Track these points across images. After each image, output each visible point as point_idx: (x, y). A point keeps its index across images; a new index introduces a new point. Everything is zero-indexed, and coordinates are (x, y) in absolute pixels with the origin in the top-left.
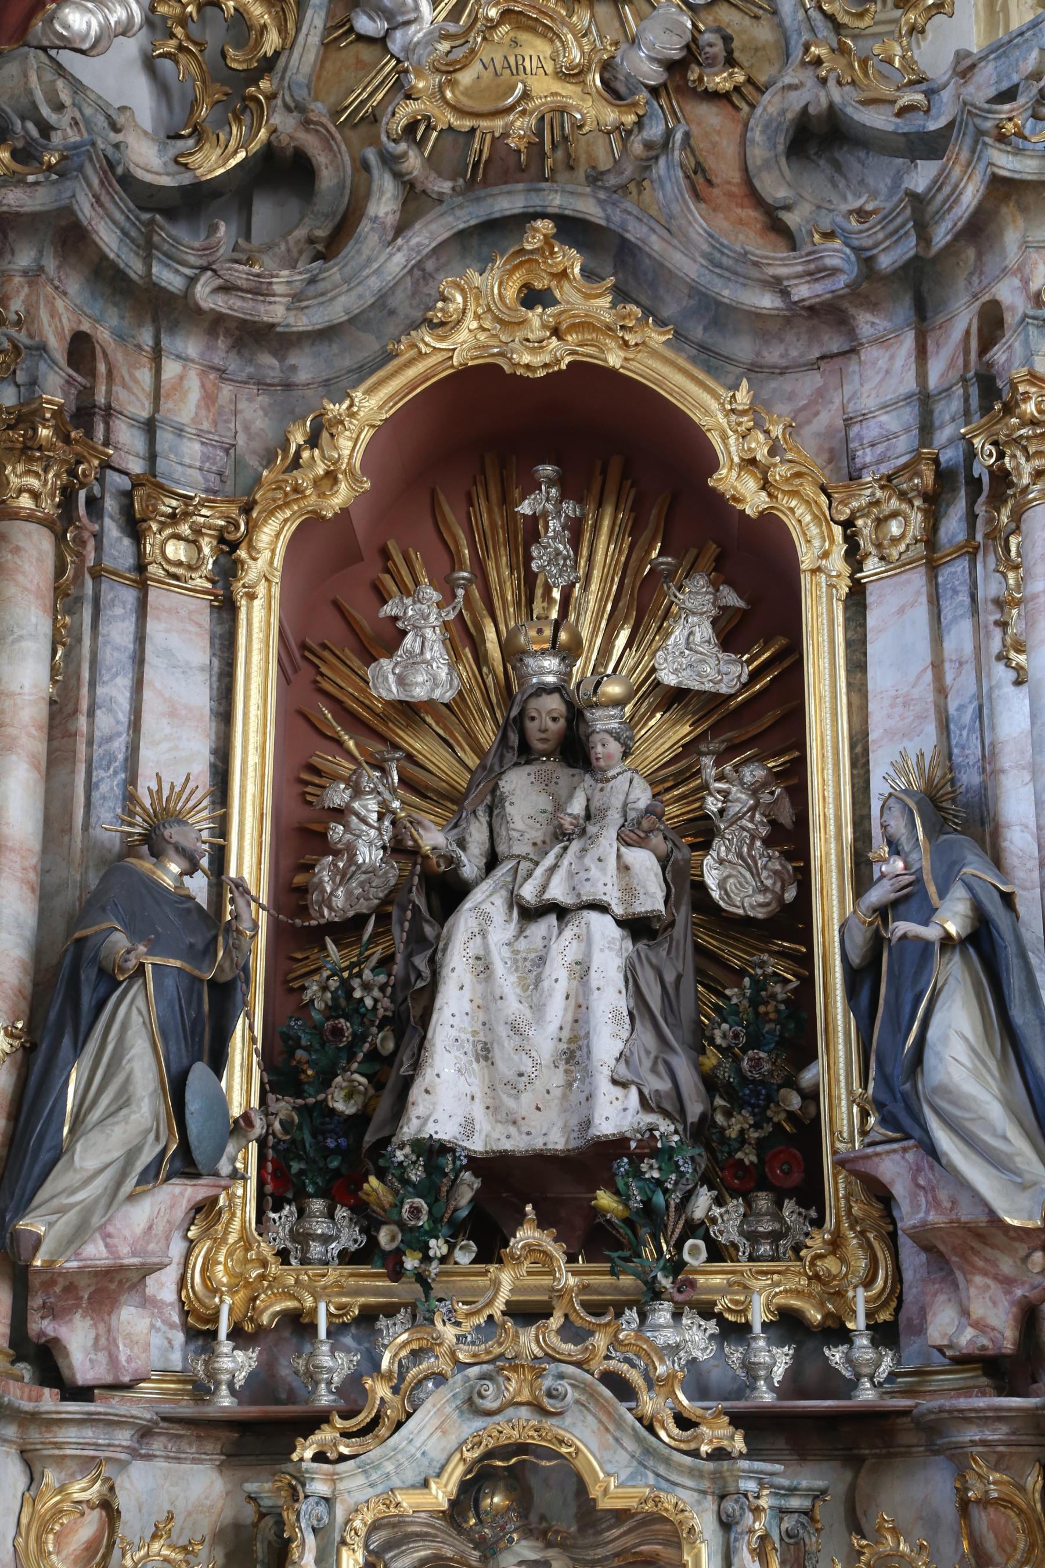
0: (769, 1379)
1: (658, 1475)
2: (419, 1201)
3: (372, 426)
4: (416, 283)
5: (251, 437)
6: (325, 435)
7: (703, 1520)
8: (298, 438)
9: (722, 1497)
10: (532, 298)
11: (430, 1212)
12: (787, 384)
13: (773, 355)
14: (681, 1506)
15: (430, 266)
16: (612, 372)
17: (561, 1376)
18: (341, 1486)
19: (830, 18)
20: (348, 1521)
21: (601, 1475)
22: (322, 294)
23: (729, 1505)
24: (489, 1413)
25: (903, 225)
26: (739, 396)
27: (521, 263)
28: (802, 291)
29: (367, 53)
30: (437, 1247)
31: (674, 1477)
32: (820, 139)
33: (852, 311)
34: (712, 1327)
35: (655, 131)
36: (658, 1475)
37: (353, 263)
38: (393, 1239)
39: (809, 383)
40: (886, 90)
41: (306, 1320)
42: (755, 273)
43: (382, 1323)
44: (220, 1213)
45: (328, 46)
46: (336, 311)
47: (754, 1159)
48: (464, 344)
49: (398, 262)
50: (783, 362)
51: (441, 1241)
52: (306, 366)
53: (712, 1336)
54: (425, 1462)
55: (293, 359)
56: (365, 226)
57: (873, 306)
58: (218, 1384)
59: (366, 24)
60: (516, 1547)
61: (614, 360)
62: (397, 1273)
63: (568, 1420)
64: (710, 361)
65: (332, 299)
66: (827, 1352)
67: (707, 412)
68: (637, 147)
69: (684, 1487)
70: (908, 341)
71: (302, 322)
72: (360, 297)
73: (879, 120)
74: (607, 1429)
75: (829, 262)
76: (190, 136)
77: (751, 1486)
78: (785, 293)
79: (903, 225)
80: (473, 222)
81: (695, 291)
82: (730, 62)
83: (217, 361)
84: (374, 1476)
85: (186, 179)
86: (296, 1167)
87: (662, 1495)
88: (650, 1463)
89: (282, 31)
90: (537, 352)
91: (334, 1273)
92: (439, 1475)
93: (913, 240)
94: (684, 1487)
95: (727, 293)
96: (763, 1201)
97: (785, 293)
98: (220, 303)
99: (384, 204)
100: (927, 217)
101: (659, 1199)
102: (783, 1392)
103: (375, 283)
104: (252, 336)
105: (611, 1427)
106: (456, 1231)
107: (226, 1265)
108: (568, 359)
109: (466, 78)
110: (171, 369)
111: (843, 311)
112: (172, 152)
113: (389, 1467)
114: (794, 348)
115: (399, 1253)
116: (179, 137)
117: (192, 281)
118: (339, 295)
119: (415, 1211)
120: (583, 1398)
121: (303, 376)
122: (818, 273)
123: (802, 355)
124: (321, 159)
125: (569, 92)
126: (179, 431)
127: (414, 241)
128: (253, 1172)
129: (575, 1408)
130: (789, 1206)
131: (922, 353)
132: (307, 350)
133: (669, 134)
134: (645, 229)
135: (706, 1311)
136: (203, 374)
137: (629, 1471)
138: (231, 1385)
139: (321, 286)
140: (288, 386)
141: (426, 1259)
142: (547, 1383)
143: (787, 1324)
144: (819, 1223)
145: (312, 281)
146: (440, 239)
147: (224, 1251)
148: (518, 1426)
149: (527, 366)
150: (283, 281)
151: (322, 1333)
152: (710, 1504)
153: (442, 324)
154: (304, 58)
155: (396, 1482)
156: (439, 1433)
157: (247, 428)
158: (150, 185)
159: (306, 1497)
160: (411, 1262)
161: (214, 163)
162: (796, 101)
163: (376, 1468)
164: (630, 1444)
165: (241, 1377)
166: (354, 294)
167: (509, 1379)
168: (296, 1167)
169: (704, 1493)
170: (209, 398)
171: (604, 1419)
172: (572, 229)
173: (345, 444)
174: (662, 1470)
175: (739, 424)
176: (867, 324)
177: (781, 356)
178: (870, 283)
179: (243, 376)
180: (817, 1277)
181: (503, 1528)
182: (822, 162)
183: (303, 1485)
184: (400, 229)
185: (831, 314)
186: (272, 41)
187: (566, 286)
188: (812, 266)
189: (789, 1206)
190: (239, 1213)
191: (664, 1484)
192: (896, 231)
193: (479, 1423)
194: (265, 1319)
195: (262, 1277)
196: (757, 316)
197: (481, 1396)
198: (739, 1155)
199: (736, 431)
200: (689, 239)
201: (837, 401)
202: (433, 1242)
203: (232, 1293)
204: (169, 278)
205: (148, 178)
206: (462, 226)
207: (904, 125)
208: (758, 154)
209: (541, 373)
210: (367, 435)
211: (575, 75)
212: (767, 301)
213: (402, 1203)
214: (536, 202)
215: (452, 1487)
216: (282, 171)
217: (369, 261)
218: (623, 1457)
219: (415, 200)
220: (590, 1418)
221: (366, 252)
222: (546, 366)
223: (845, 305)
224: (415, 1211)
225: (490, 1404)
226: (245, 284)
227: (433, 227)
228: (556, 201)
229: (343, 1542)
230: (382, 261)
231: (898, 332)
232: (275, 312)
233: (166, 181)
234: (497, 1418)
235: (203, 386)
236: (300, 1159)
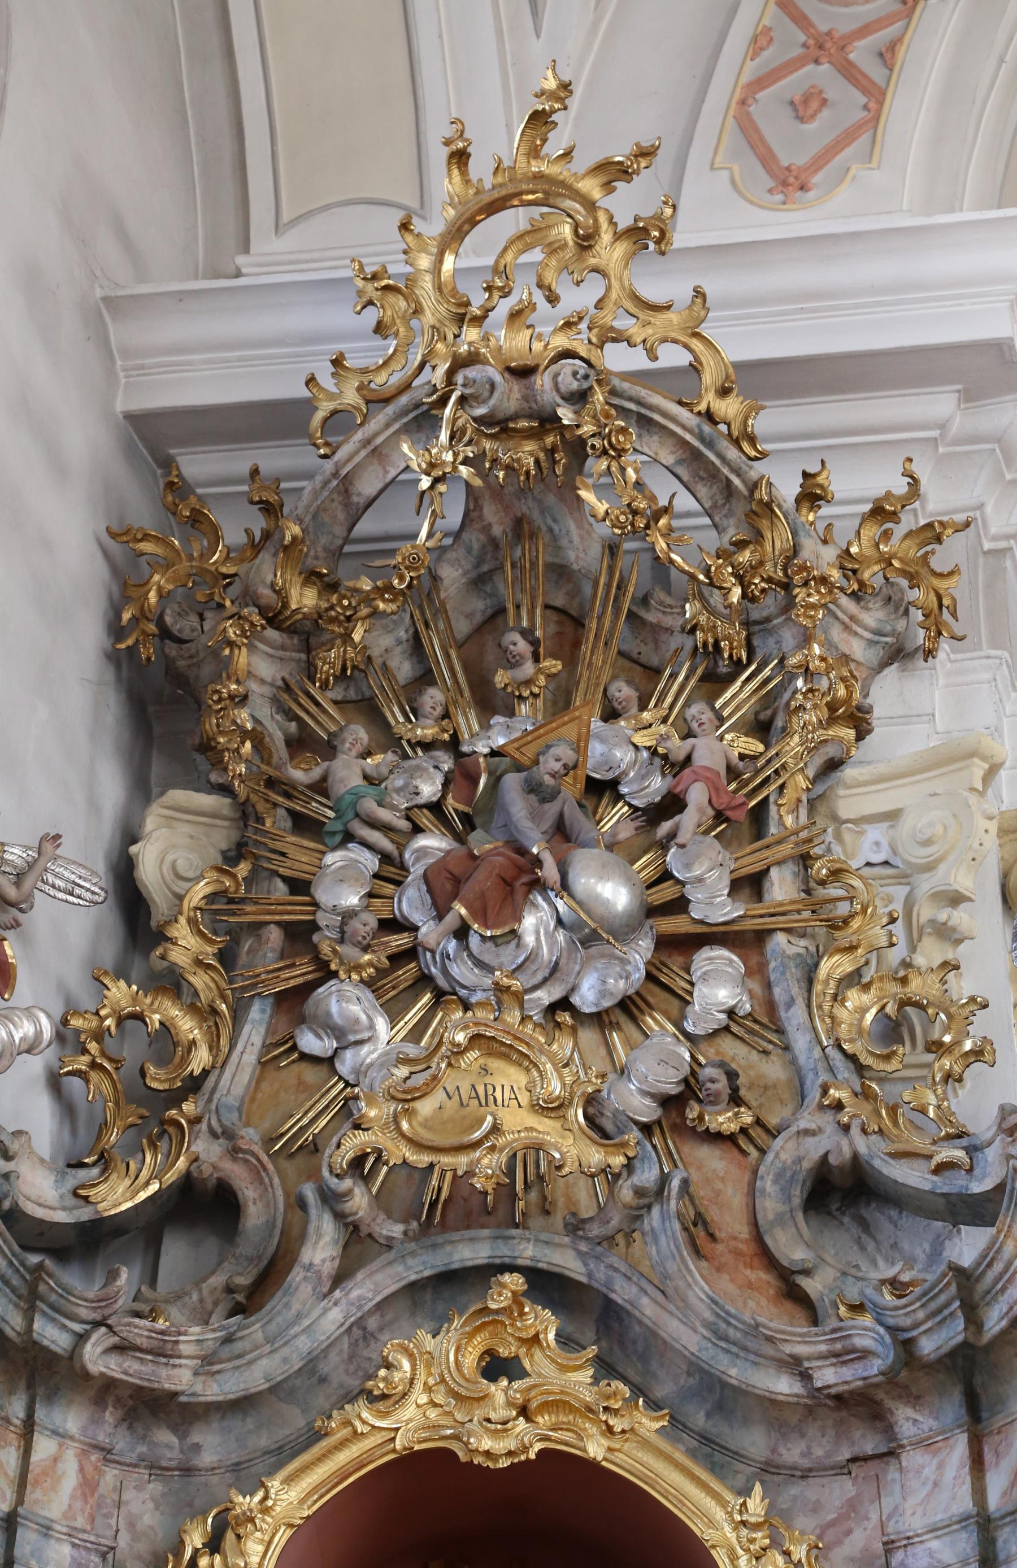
3: (290, 1526)
4: (354, 1344)
5: (135, 1537)
6: (230, 1536)
8: (195, 1539)
10: (496, 1367)
12: (811, 1490)
13: (792, 1453)
15: (372, 1323)
16: (592, 1467)
19: (852, 1058)
22: (239, 1356)
25: (948, 1304)
26: (751, 1504)
27: (484, 1325)
28: (827, 1376)
29: (310, 1074)
32: (841, 1192)
33: (889, 1403)
35: (647, 1176)
37: (279, 1319)
39: (838, 1491)
40: (920, 1143)
42: (769, 1350)
45: (266, 1064)
46: (254, 1378)
48: (410, 1423)
49: (333, 1318)
50: (806, 1463)
52: (212, 1445)
55: (195, 1437)
56: (297, 1275)
57: (915, 1399)
59: (310, 1042)
61: (595, 1449)
64: (714, 1455)
65: (250, 1363)
67: (712, 1523)
68: (626, 1193)
70: (960, 1447)
71: (212, 1391)
72: (285, 1360)
73: (912, 1176)
75: (860, 1342)
76: (95, 1164)
78: (805, 1376)
79: (948, 1304)
80: (427, 1273)
81: (696, 1368)
82: (736, 1100)
83: (102, 1437)
85: (85, 1214)
89: (214, 1047)
90: (499, 1437)
93: (960, 1324)
95: (735, 1372)
97: (805, 1376)
98: (113, 1367)
99: (321, 1249)
100: (977, 1297)
103: (304, 1344)
104: (148, 1407)
108: (538, 1446)
109: (425, 1107)
110: (43, 1447)
111: (879, 1403)
112: (71, 1183)
114: (815, 1445)
116: (81, 1165)
117: (81, 1338)
118: (260, 1357)
121: (207, 1458)
122: (846, 1355)
123: (828, 1455)
124: (248, 1192)
125: (546, 1128)
126: (46, 1530)
127: (355, 1294)
131: (977, 1463)
132: (215, 1425)
133: (664, 1180)
134: (634, 1290)
136: (83, 1454)
139: (238, 1346)
140: (187, 1471)
145: (228, 1340)
146: (386, 1292)
149: (487, 1453)
150: (193, 1338)
153: (384, 1397)
154: (237, 1078)
157: (131, 1525)
158: (42, 1222)
161: (119, 1196)
162: (814, 1149)
166: (277, 1357)
170: (88, 1485)
172: (546, 1286)
173: (254, 1548)
175: (752, 1541)
176: (909, 1421)
177: (803, 1455)
178: (909, 1372)
179: (132, 1457)
182: (846, 1220)
184: (339, 1279)
185: (862, 1405)
186: (201, 1059)
187: (538, 1354)
188: (838, 1346)
192: (939, 1311)
196: (771, 1403)
199: (747, 1551)
200: (689, 1304)
201: (874, 1517)
204: (53, 1335)
205: (39, 1213)
206: (413, 1277)
207: (943, 1184)
208: (770, 1206)
209: (504, 1463)
210: (283, 1536)
211: (553, 1109)
212: (785, 1386)
214: (503, 1252)
216: (202, 1206)
217: (299, 1316)
219: (358, 1245)
221: (296, 1306)
222: (510, 1453)
223: (880, 1395)
226: (145, 1346)
227: (379, 1277)
228: (527, 1252)
230: (313, 1317)
231: (947, 1433)
232: (180, 1378)
233: (61, 1217)
235: (81, 1470)
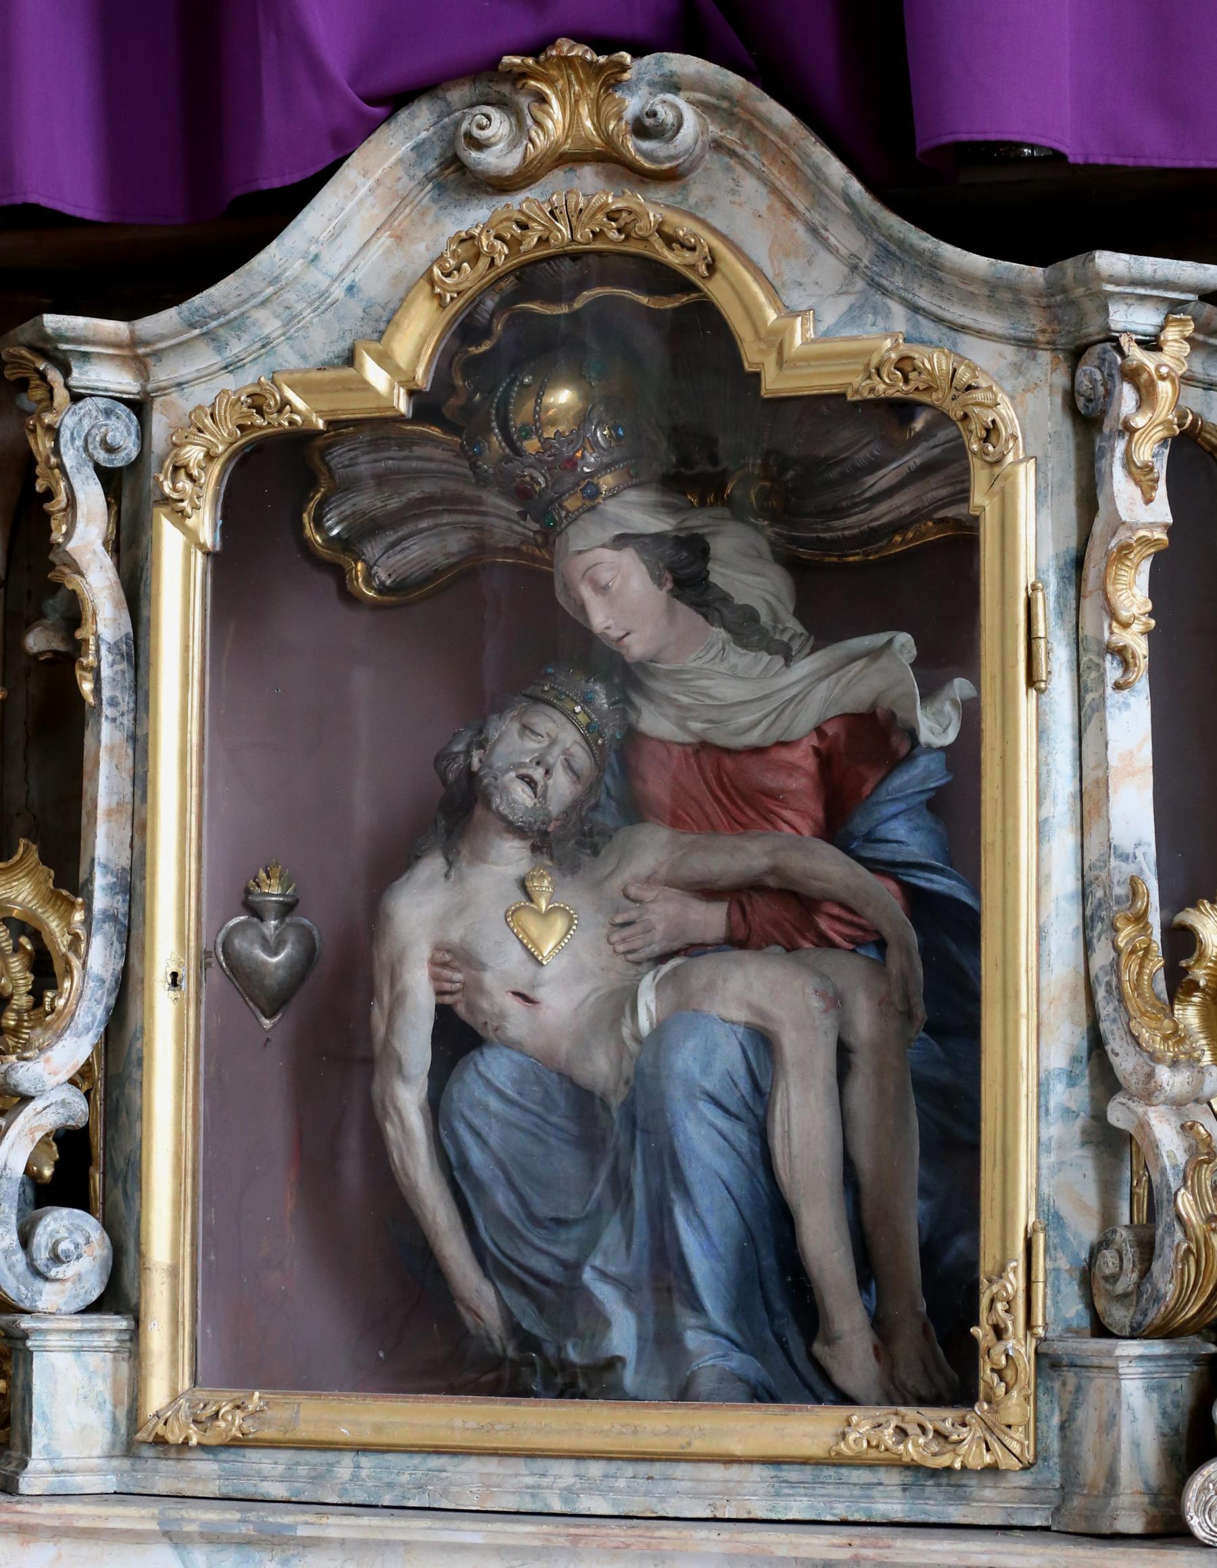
1: (916, 309)
7: (1017, 404)
9: (1076, 355)
14: (964, 376)
18: (162, 374)
21: (771, 315)
24: (501, 185)
31: (955, 312)
36: (916, 309)
54: (355, 308)
60: (610, 507)
69: (980, 333)
74: (790, 207)
84: (236, 348)
87: (920, 355)
88: (897, 281)
94: (980, 333)
105: (800, 203)
113: (268, 323)
129: (712, 160)
137: (844, 303)
142: (633, 104)
152: (1047, 373)
156: (385, 240)
159: (76, 398)
164: (844, 237)
167: (542, 99)
169: (1028, 344)
171: (782, 182)
174: (924, 298)
183: (66, 372)
191: (930, 330)
193: (476, 215)
218: (829, 269)
220: (750, 184)
225: (500, 157)
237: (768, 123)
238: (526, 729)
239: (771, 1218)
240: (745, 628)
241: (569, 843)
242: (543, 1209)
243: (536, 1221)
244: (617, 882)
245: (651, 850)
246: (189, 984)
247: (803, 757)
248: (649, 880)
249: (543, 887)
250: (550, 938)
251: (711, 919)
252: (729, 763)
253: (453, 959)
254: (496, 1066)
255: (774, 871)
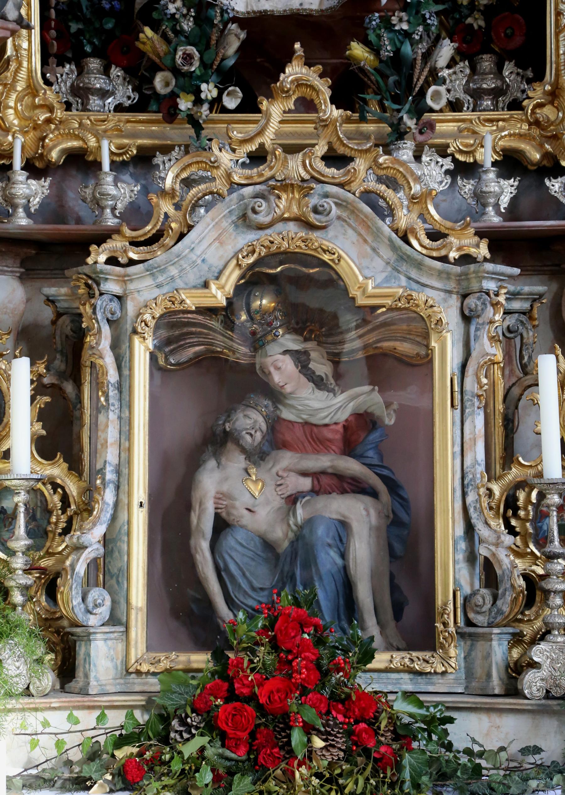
0: (497, 206)
1: (410, 278)
2: (192, 49)
7: (449, 313)
9: (464, 296)
11: (201, 59)
14: (431, 302)
17: (326, 195)
18: (131, 287)
20: (139, 314)
21: (361, 278)
23: (471, 301)
24: (261, 227)
30: (209, 91)
31: (424, 280)
34: (448, 164)
36: (410, 278)
38: (167, 84)
41: (91, 158)
43: (159, 159)
44: (8, 61)
47: (482, 23)
51: (211, 86)
53: (447, 172)
54: (205, 267)
58: (15, 207)
60: (281, 340)
62: (171, 114)
63: (331, 232)
66: (547, 182)
69: (432, 288)
74: (365, 241)
77: (491, 285)
84: (161, 279)
86: (74, 27)
87: (414, 294)
88: (404, 267)
91: (115, 118)
92: (217, 278)
94: (432, 288)
96: (486, 63)
101: (407, 49)
102: (513, 212)
105: (369, 239)
106: (226, 79)
107: (16, 109)
115: (173, 96)
119: (188, 58)
120: (344, 215)
128: (36, 21)
129: (337, 223)
130: (508, 69)
135: (442, 151)
137: (384, 275)
138: (27, 209)
141: (198, 102)
142: (313, 201)
143: (509, 163)
144: (539, 76)
147: (14, 96)
148: (289, 237)
151: (106, 166)
152: (455, 301)
155: (179, 283)
156: (217, 244)
159: (101, 294)
160: (185, 104)
163: (163, 271)
164: (386, 253)
165: (35, 202)
167: (279, 198)
168: (74, 27)
171: (363, 232)
174: (414, 274)
180: (537, 123)
181: (270, 324)
183: (98, 284)
189: (508, 69)
190: (25, 64)
191: (415, 286)
193: (251, 236)
194: (54, 155)
195: (48, 121)
197: (254, 211)
198: (469, 20)
202: (204, 86)
203: (24, 133)
213: (175, 50)
215: (230, 288)
218: (379, 263)
220: (350, 232)
224: (188, 58)
225: (263, 218)
229: (135, 332)
234: (269, 231)
236: (78, 20)
237: (361, 211)
238: (246, 416)
239: (347, 586)
240: (319, 383)
241: (257, 456)
242: (257, 585)
243: (253, 589)
244: (274, 470)
245: (286, 459)
246: (146, 506)
247: (340, 428)
248: (285, 470)
249: (253, 471)
250: (255, 489)
251: (306, 483)
252: (315, 429)
253: (220, 496)
254: (240, 535)
255: (331, 467)
